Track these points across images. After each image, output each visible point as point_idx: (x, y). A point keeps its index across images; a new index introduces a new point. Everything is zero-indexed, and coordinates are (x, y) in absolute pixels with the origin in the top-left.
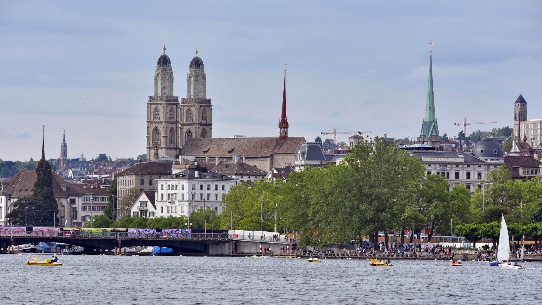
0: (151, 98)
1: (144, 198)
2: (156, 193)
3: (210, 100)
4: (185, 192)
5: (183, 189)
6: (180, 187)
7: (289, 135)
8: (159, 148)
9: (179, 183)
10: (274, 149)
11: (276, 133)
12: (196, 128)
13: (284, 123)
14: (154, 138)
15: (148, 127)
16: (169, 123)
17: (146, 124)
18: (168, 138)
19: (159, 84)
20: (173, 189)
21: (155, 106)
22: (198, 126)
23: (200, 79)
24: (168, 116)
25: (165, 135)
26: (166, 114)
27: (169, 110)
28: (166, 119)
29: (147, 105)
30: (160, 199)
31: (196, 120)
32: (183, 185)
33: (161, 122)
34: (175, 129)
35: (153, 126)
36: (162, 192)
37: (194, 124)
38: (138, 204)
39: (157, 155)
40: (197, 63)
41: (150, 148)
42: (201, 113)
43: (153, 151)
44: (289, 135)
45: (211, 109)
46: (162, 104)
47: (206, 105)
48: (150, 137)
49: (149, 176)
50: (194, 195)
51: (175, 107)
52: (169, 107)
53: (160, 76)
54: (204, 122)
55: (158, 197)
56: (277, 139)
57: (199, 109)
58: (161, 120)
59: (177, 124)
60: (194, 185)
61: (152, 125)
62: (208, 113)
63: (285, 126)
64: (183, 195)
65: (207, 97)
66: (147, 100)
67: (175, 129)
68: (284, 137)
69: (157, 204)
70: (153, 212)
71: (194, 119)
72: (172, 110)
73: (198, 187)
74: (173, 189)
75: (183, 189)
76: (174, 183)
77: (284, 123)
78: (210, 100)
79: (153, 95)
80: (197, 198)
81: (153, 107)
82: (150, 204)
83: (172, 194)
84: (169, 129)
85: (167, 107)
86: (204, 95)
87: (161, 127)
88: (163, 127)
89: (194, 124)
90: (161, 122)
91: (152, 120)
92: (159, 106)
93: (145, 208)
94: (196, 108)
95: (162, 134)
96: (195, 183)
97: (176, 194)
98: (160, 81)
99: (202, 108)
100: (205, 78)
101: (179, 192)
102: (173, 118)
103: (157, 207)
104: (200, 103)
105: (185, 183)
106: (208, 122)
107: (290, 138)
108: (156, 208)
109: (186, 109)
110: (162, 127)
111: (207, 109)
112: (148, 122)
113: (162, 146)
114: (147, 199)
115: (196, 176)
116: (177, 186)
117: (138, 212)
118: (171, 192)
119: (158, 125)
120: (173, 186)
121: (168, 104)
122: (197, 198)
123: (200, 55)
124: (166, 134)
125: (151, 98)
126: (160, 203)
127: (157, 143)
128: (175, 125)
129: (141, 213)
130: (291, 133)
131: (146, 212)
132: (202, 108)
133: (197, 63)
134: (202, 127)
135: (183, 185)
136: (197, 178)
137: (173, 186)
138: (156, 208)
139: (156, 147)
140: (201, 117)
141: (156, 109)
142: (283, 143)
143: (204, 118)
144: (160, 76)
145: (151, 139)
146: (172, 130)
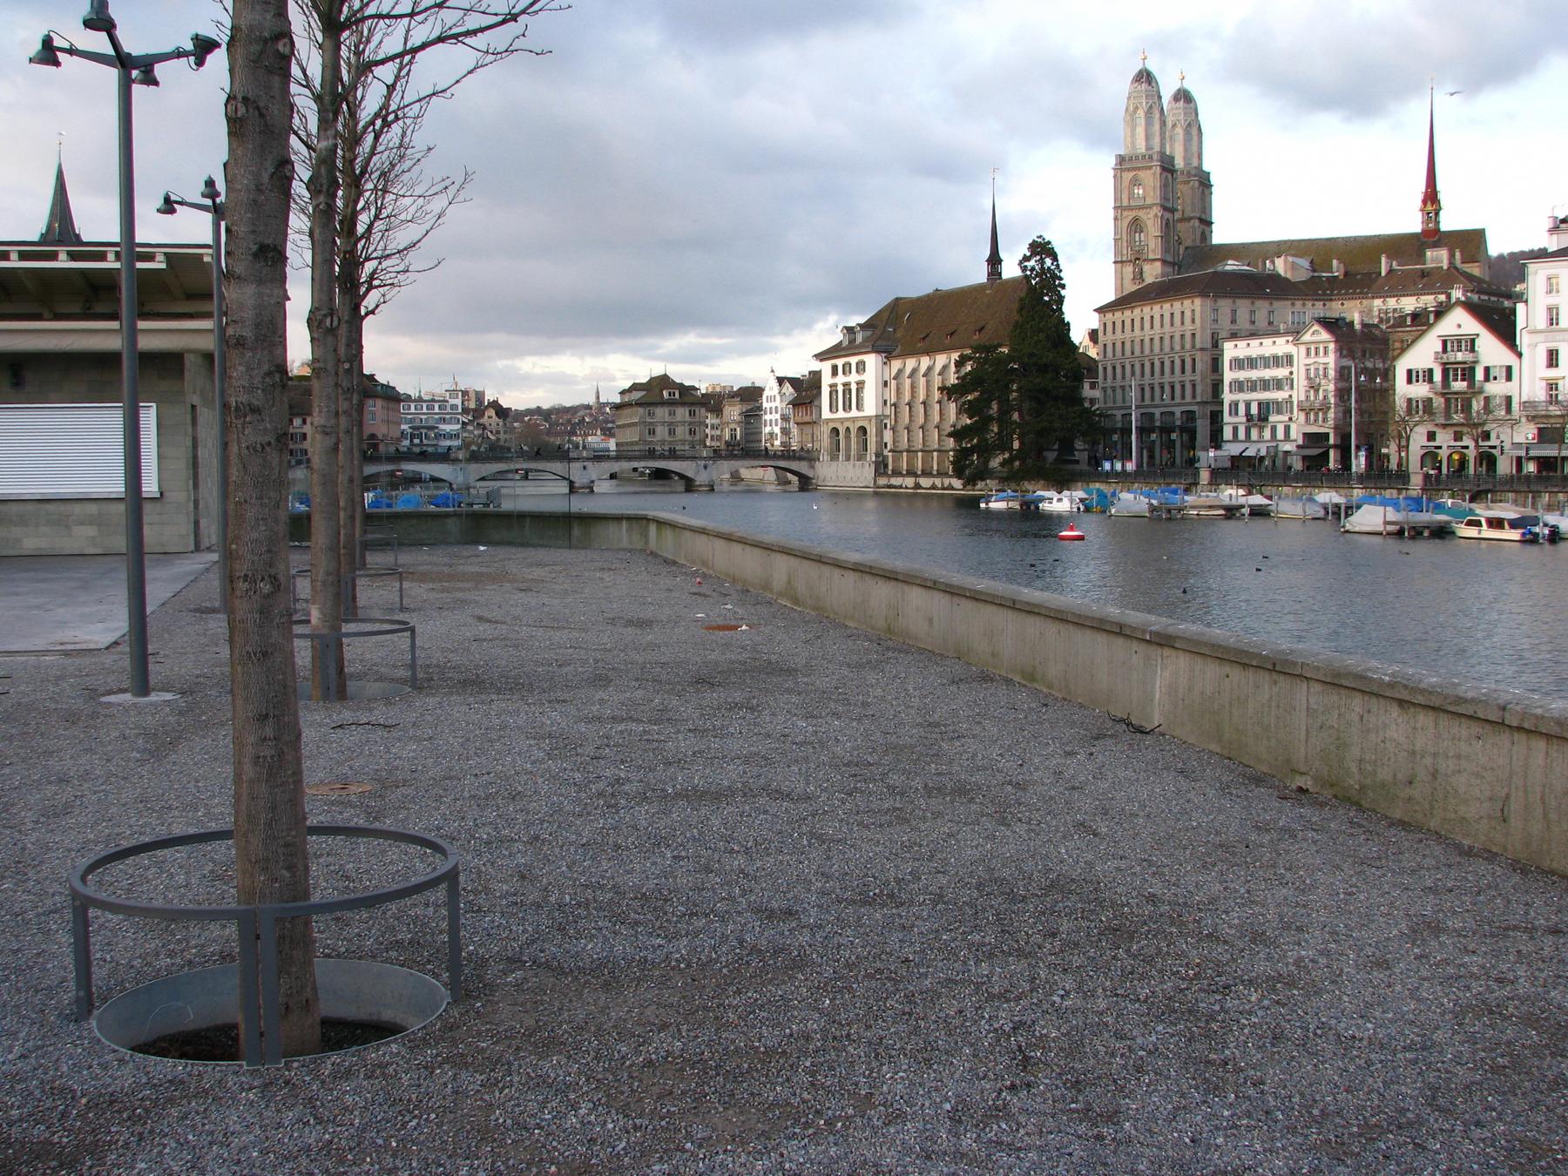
2: (1520, 307)
11: (1411, 223)
14: (1131, 243)
15: (1116, 219)
21: (1131, 174)
22: (1197, 223)
23: (1194, 131)
29: (1112, 173)
30: (1541, 321)
33: (1150, 207)
35: (1130, 215)
37: (1189, 219)
39: (1139, 275)
40: (1184, 96)
43: (1129, 269)
69: (1523, 339)
70: (1509, 369)
81: (1128, 176)
86: (1200, 164)
89: (1189, 219)
90: (1150, 207)
91: (1125, 203)
92: (1141, 174)
93: (1460, 356)
112: (1115, 208)
113: (1151, 256)
117: (1431, 371)
119: (1141, 214)
123: (1188, 86)
126: (1540, 337)
129: (1445, 373)
131: (1472, 370)
138: (1520, 355)
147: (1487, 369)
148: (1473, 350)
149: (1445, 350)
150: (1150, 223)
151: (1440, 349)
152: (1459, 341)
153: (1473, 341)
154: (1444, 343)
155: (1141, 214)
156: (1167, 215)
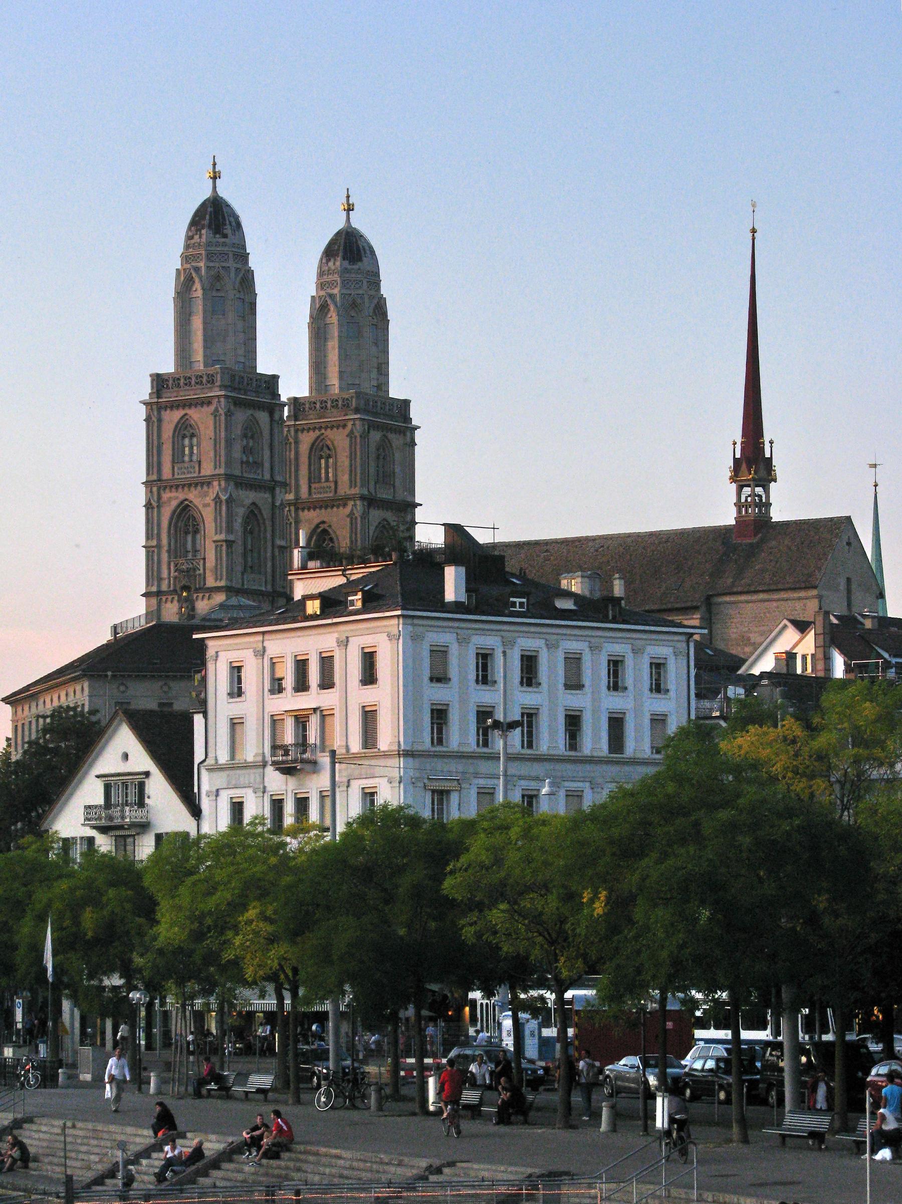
0: (159, 382)
1: (124, 751)
3: (406, 403)
4: (386, 695)
5: (369, 677)
6: (349, 667)
7: (777, 515)
8: (197, 590)
9: (344, 643)
10: (717, 573)
12: (351, 515)
13: (753, 464)
14: (178, 551)
15: (148, 506)
16: (241, 483)
17: (140, 496)
18: (239, 548)
19: (197, 323)
20: (302, 685)
24: (237, 453)
25: (222, 537)
26: (229, 443)
27: (238, 431)
28: (228, 464)
29: (142, 411)
31: (352, 483)
32: (369, 660)
34: (266, 513)
35: (173, 499)
36: (235, 708)
38: (89, 792)
41: (159, 593)
42: (373, 456)
44: (777, 515)
45: (413, 444)
46: (207, 402)
47: (390, 427)
48: (159, 546)
49: (156, 685)
50: (440, 715)
51: (263, 417)
52: (241, 416)
53: (197, 285)
54: (384, 494)
55: (209, 740)
56: (720, 534)
57: (365, 436)
58: (208, 469)
59: (272, 490)
60: (439, 654)
61: (166, 495)
62: (398, 456)
63: (762, 473)
64: (369, 717)
65: (396, 391)
66: (145, 390)
67: (266, 513)
68: (755, 523)
69: (205, 782)
71: (344, 478)
72: (251, 432)
73: (462, 664)
74: (302, 685)
75: (369, 677)
76: (312, 643)
77: (753, 464)
78: (406, 403)
79: (168, 367)
80: (462, 734)
81: (172, 418)
82: (160, 791)
83: (301, 720)
84: (241, 512)
85: (229, 414)
87: (204, 503)
88: (217, 499)
93: (131, 815)
94: (351, 435)
95: (211, 534)
96: (446, 638)
97: (324, 716)
98: (198, 308)
99: (375, 436)
100: (385, 314)
101: (347, 698)
102: (258, 464)
103: (206, 804)
104: (366, 411)
105: (384, 636)
106: (401, 495)
107: (785, 525)
108: (196, 812)
109: (306, 439)
110: (209, 500)
111: (396, 440)
113: (211, 582)
114: (141, 760)
115: (450, 595)
116: (326, 662)
118: (290, 701)
119: (193, 496)
120: (301, 666)
121: (238, 403)
122: (462, 734)
123: (358, 222)
124: (230, 530)
125: (159, 382)
126: (220, 779)
127: (190, 573)
128: (267, 495)
130: (786, 505)
132: (375, 436)
133: (349, 251)
134: (376, 515)
135: (369, 660)
136: (457, 607)
137: (301, 666)
138: (196, 812)
139: (186, 588)
140: (372, 470)
141: (184, 430)
142: (752, 551)
143: (385, 477)
144: (197, 285)
145: (165, 556)
146: (253, 514)
147: (159, 837)
148: (141, 804)
149: (108, 804)
150: (208, 515)
151: (101, 801)
152: (125, 785)
153: (141, 786)
154: (107, 788)
155: (193, 496)
156: (249, 497)
